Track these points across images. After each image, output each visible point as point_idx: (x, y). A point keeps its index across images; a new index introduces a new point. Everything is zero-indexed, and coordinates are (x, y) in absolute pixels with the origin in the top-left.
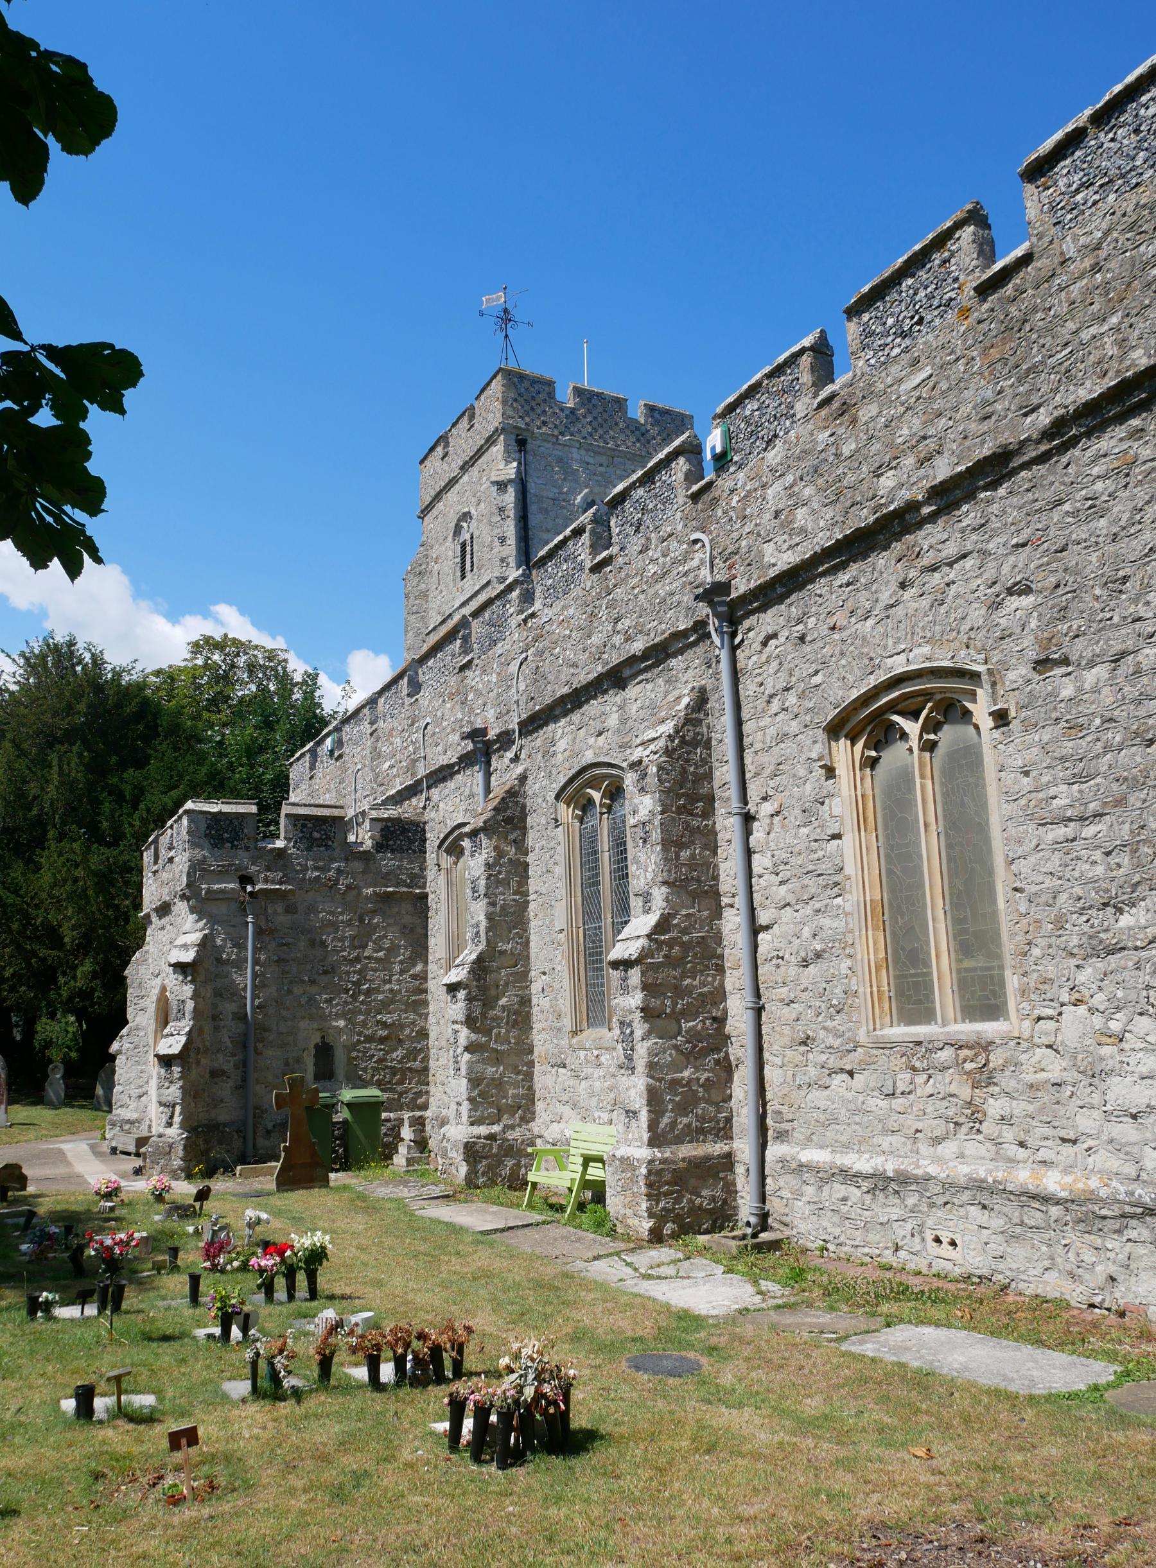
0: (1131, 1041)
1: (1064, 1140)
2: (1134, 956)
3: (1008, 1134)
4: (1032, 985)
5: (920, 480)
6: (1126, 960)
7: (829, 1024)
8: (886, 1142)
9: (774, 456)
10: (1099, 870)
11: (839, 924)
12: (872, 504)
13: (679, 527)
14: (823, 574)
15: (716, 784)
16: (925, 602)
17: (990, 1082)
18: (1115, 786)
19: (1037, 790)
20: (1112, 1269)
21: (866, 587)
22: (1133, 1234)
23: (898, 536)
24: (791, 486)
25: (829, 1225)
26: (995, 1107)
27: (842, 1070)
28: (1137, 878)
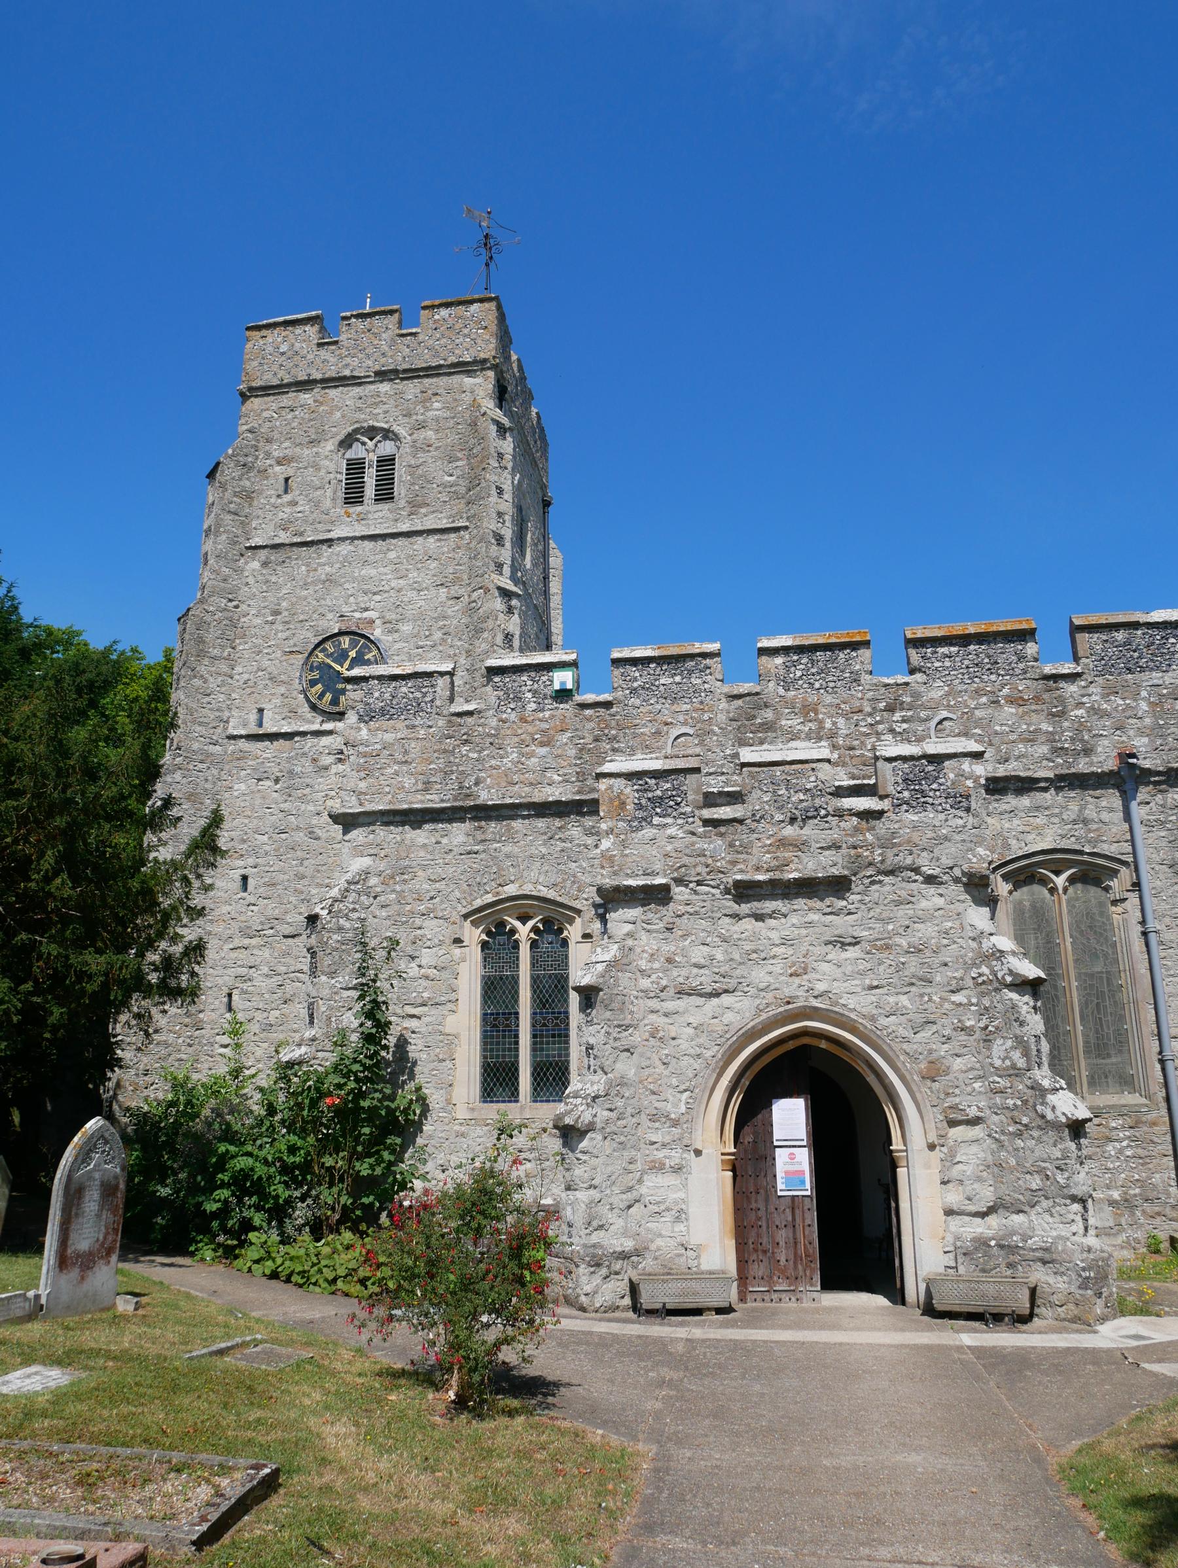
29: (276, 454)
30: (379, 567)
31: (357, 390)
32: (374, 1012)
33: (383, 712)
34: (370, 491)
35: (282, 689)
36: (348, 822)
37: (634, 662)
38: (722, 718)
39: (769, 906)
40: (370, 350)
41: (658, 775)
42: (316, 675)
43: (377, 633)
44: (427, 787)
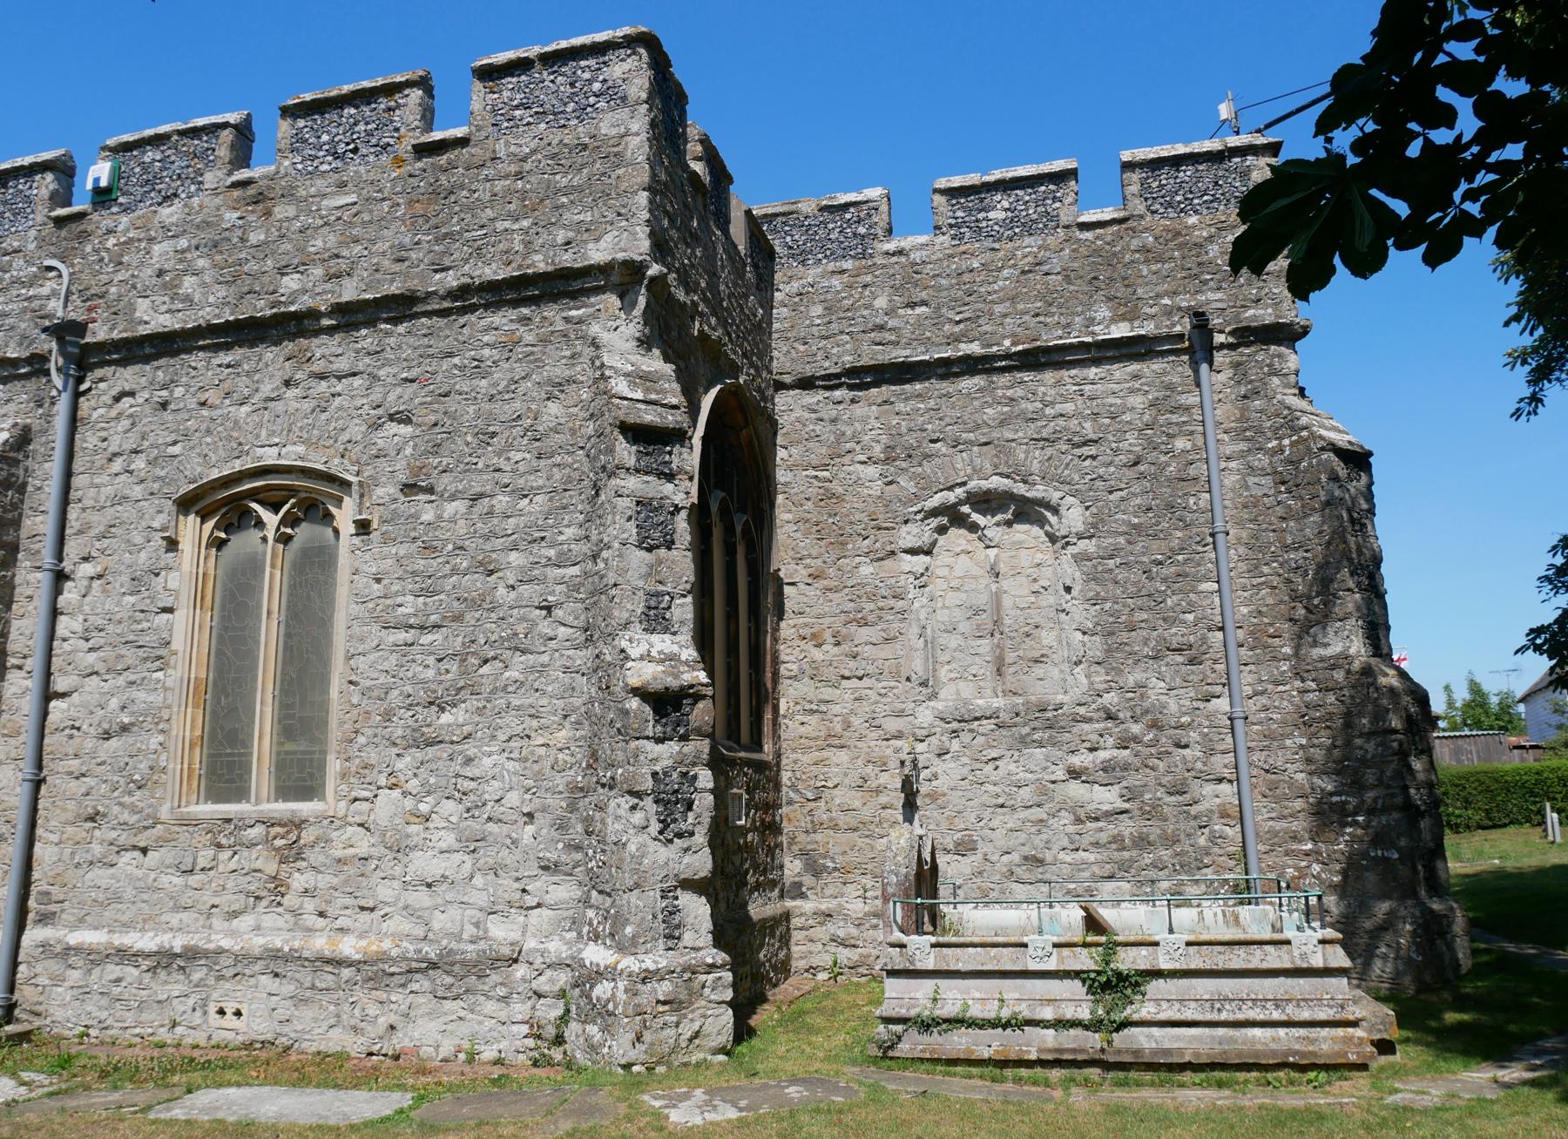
0: (436, 821)
1: (363, 909)
2: (449, 748)
3: (310, 905)
4: (353, 769)
5: (325, 292)
6: (442, 751)
7: (127, 799)
8: (175, 919)
9: (170, 214)
10: (430, 673)
11: (157, 699)
12: (272, 298)
13: (32, 246)
14: (202, 348)
15: (24, 533)
16: (307, 406)
17: (299, 857)
18: (456, 604)
19: (385, 597)
20: (393, 1018)
21: (248, 374)
22: (415, 986)
23: (293, 337)
24: (183, 251)
25: (95, 1009)
26: (299, 881)
27: (135, 847)
28: (461, 683)
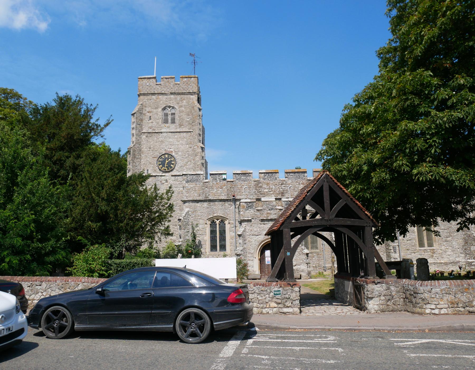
11: (414, 237)
26: (435, 255)
29: (147, 110)
30: (173, 139)
31: (166, 96)
32: (194, 237)
33: (190, 181)
34: (170, 121)
35: (153, 166)
36: (185, 202)
37: (237, 174)
38: (253, 185)
39: (266, 222)
40: (168, 87)
41: (249, 202)
42: (160, 163)
43: (173, 154)
44: (200, 195)
